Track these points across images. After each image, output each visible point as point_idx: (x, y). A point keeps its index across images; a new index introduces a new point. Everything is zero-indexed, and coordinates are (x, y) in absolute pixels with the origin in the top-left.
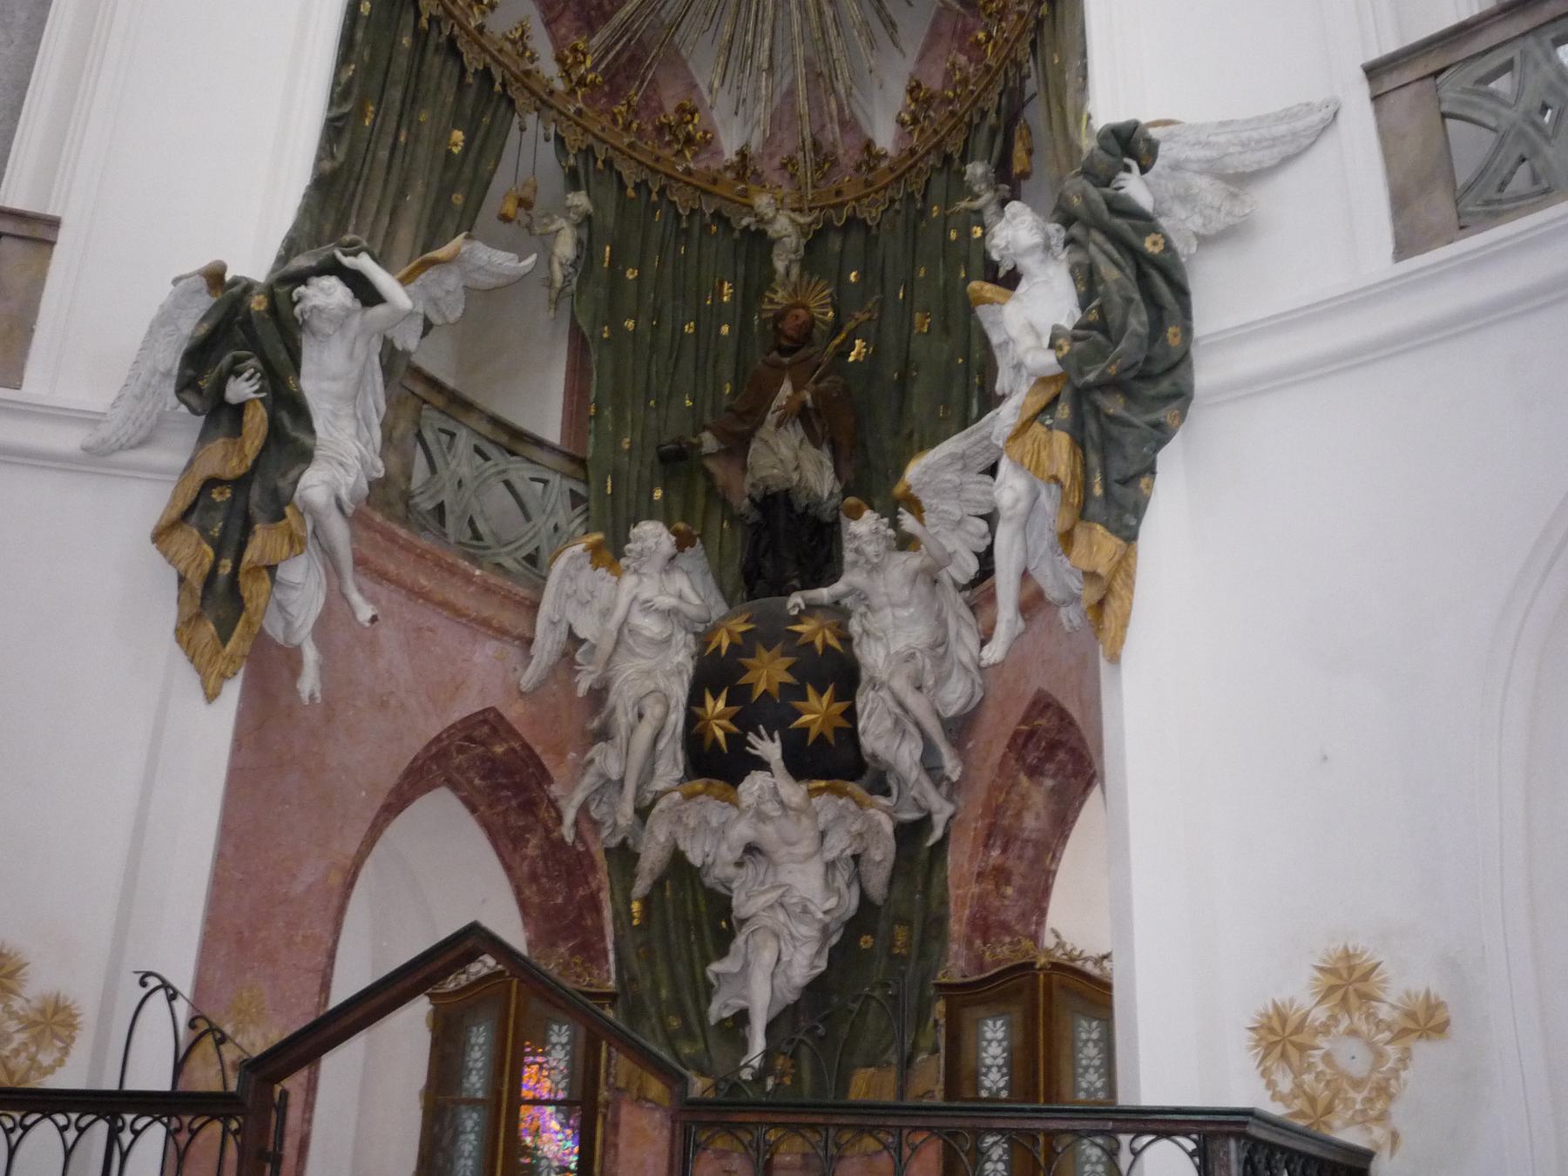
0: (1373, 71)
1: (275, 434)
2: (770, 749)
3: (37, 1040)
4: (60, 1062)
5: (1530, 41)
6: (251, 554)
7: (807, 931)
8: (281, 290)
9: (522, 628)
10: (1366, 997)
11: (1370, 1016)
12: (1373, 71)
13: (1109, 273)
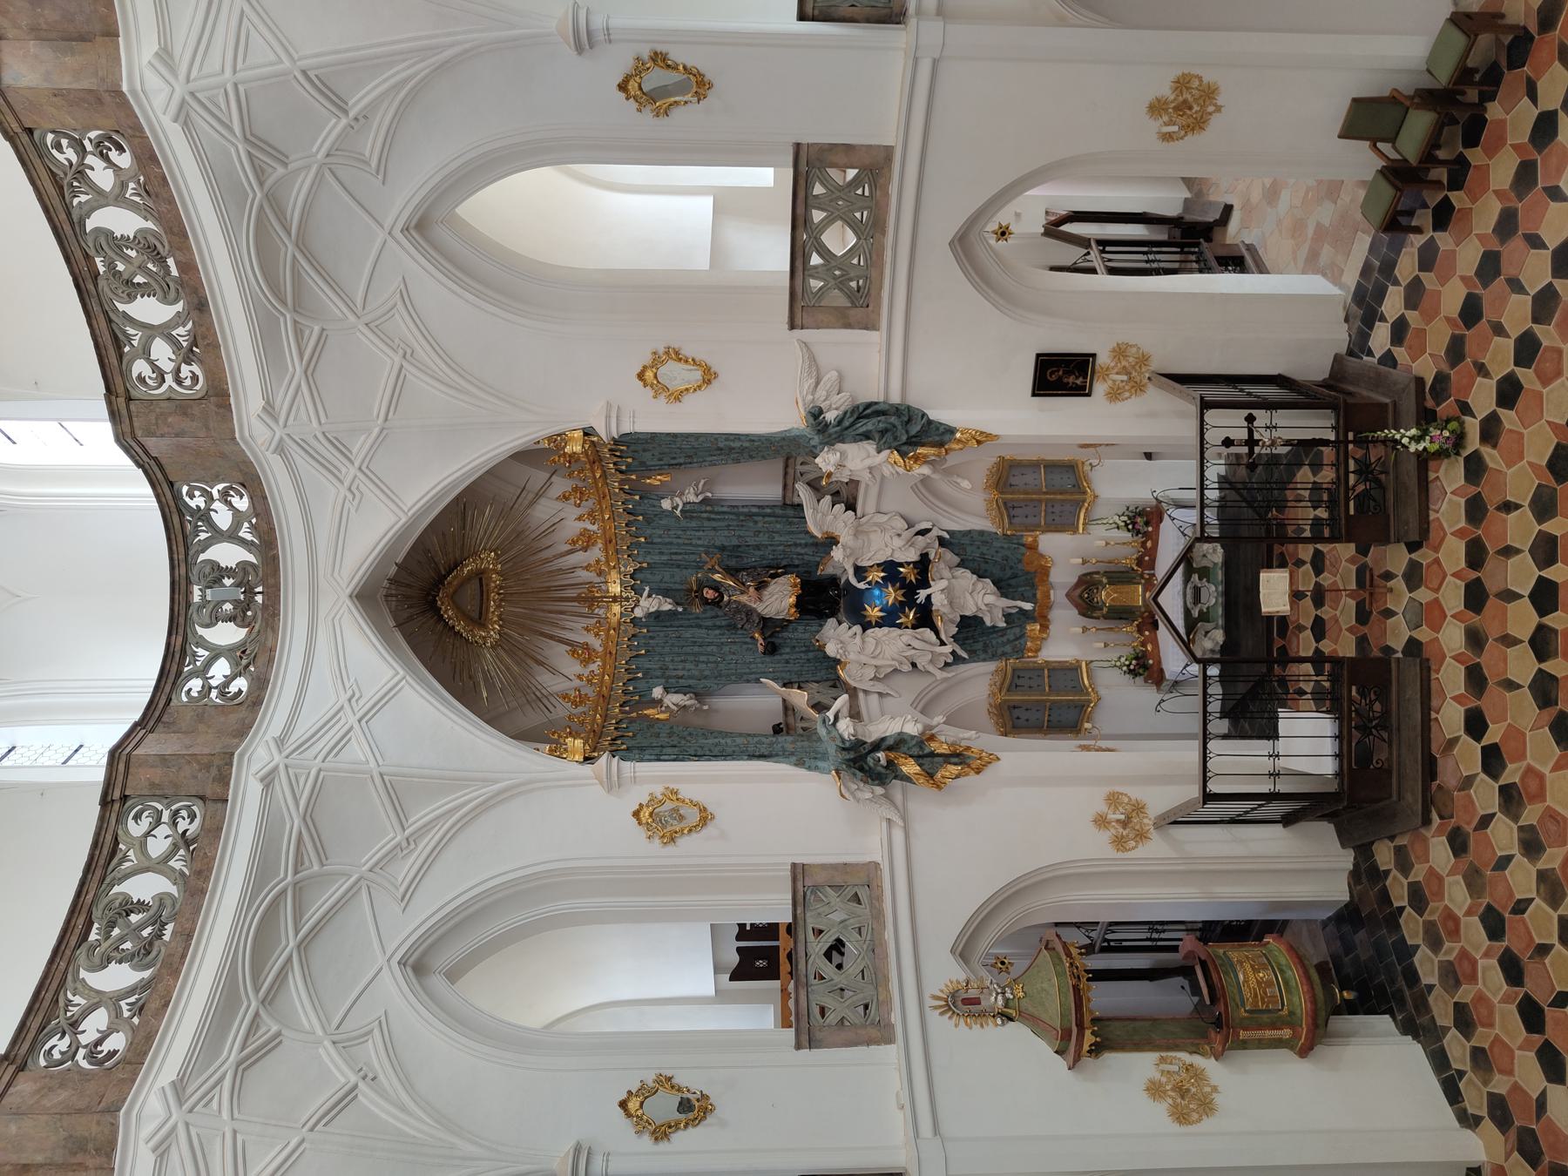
0: (792, 326)
1: (890, 749)
2: (922, 595)
3: (1121, 804)
4: (1126, 795)
5: (806, 273)
6: (944, 749)
7: (980, 585)
8: (847, 745)
9: (876, 696)
10: (1108, 369)
11: (1113, 368)
12: (792, 326)
13: (870, 426)
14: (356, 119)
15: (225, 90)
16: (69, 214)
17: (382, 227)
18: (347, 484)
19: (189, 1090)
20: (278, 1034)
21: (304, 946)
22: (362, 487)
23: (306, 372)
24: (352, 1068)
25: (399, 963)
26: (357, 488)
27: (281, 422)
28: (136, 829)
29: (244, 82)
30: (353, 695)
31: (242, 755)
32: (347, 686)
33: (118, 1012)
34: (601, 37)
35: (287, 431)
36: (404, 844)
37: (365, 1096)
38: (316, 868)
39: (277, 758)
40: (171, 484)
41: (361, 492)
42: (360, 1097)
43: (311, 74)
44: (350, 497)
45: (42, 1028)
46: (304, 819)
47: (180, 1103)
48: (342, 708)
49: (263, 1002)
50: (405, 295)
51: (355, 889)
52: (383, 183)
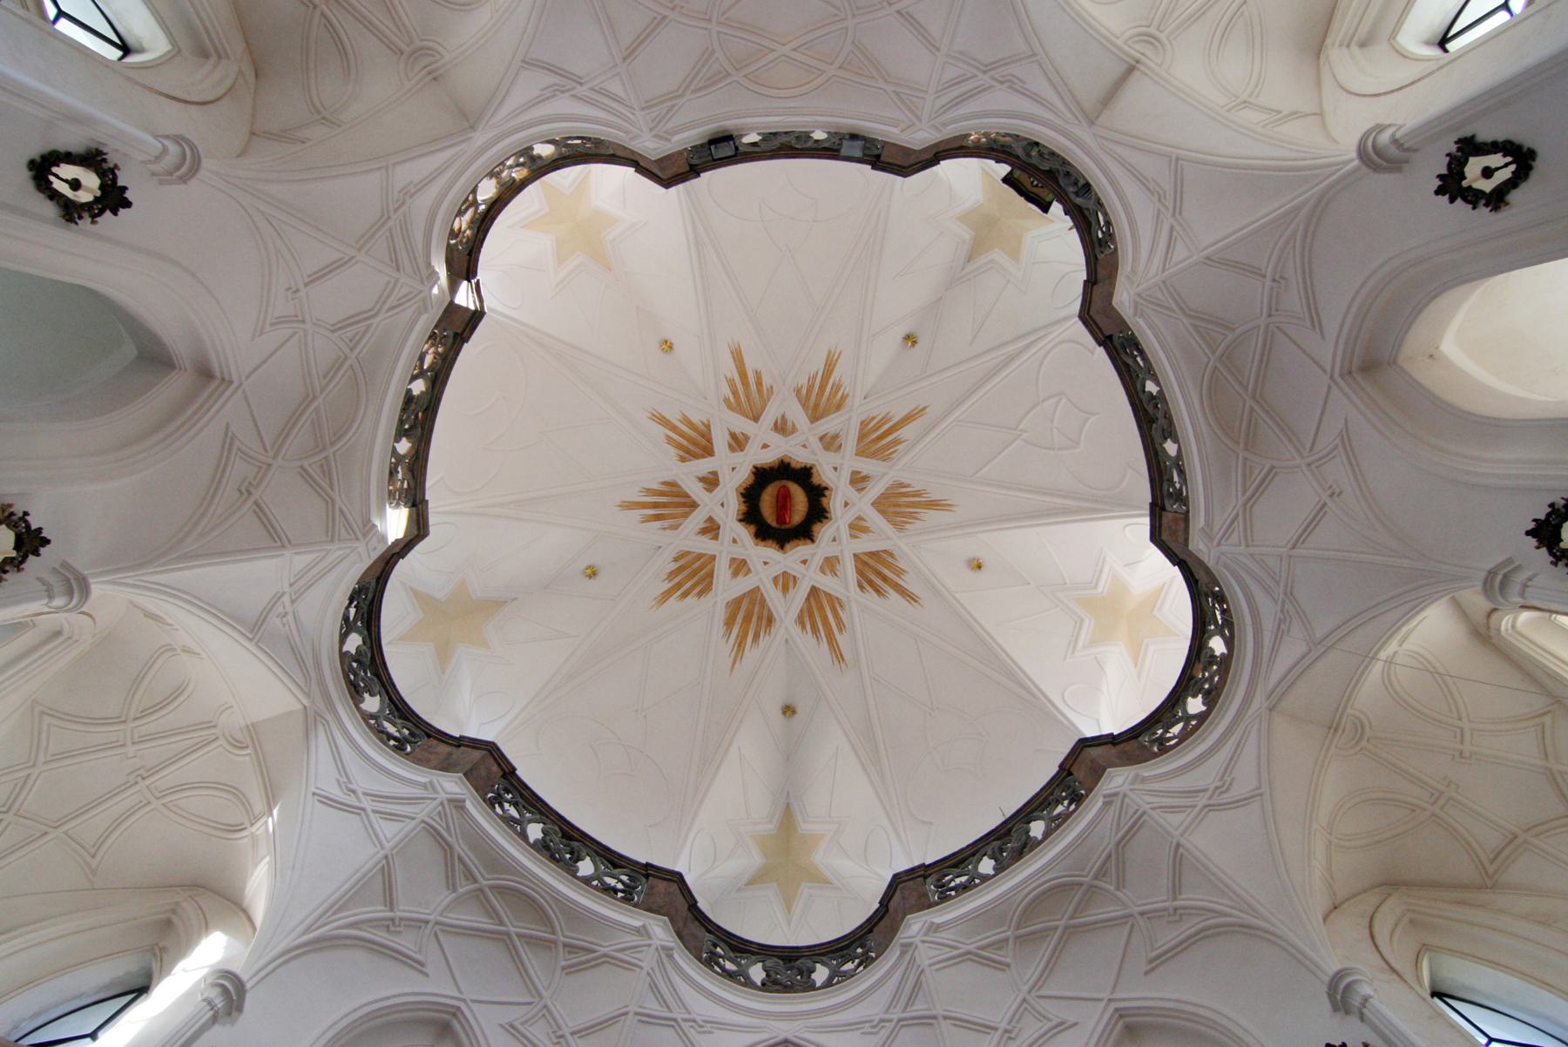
14: (1176, 909)
15: (1137, 810)
16: (1032, 812)
17: (1113, 991)
18: (887, 1016)
19: (454, 811)
20: (455, 890)
21: (503, 938)
22: (883, 1031)
23: (969, 953)
24: (401, 919)
25: (459, 1008)
26: (883, 1027)
27: (925, 938)
28: (624, 878)
29: (1149, 816)
30: (701, 1026)
31: (665, 922)
32: (709, 1025)
33: (513, 819)
34: (1356, 1002)
35: (920, 944)
36: (560, 1033)
37: (381, 911)
38: (563, 963)
39: (658, 943)
40: (870, 931)
41: (876, 1033)
42: (383, 908)
43: (1181, 850)
44: (875, 1023)
45: (522, 795)
46: (605, 955)
47: (450, 801)
48: (689, 1013)
49: (481, 890)
50: (1062, 1026)
51: (534, 992)
52: (1146, 973)
